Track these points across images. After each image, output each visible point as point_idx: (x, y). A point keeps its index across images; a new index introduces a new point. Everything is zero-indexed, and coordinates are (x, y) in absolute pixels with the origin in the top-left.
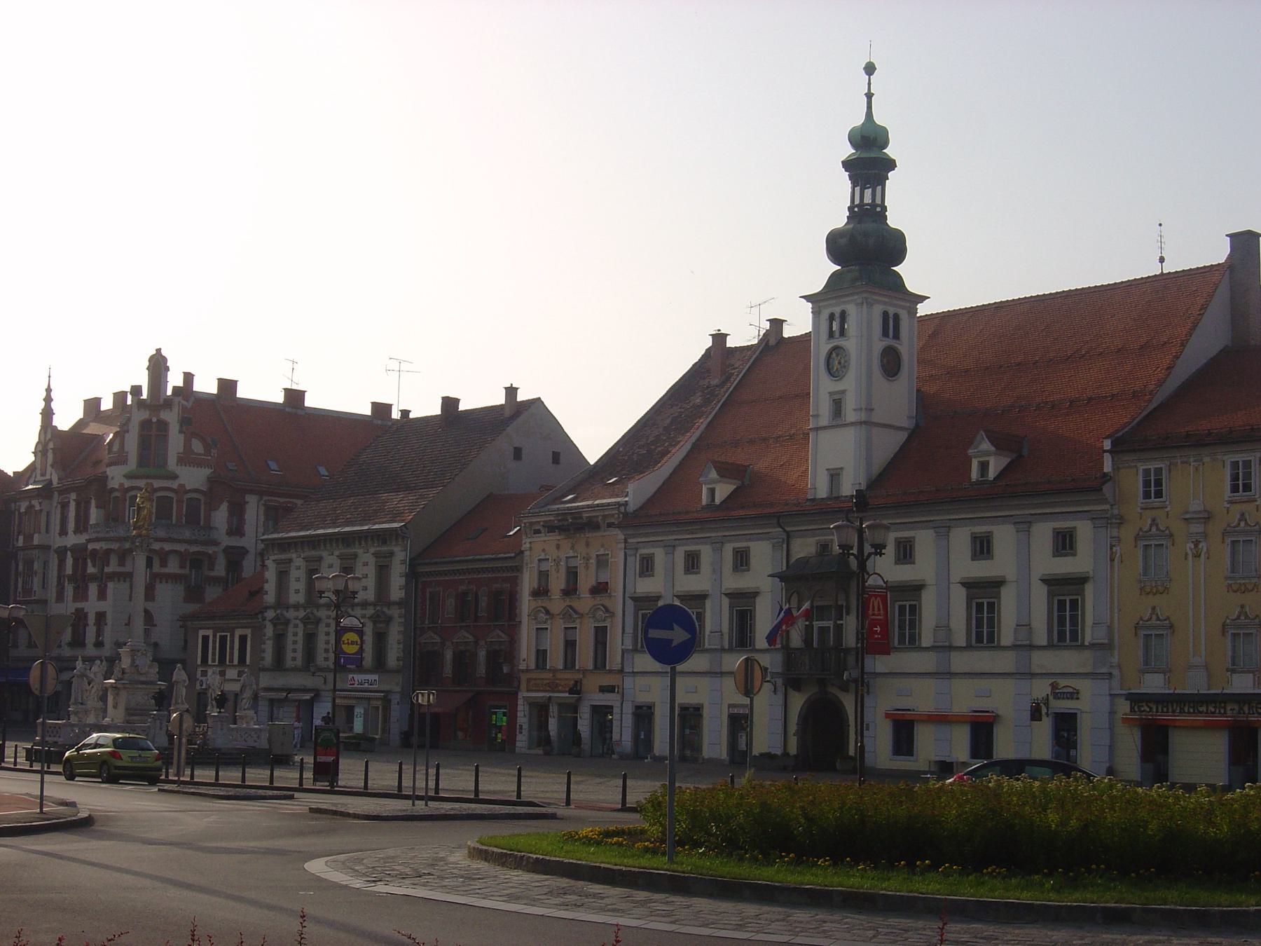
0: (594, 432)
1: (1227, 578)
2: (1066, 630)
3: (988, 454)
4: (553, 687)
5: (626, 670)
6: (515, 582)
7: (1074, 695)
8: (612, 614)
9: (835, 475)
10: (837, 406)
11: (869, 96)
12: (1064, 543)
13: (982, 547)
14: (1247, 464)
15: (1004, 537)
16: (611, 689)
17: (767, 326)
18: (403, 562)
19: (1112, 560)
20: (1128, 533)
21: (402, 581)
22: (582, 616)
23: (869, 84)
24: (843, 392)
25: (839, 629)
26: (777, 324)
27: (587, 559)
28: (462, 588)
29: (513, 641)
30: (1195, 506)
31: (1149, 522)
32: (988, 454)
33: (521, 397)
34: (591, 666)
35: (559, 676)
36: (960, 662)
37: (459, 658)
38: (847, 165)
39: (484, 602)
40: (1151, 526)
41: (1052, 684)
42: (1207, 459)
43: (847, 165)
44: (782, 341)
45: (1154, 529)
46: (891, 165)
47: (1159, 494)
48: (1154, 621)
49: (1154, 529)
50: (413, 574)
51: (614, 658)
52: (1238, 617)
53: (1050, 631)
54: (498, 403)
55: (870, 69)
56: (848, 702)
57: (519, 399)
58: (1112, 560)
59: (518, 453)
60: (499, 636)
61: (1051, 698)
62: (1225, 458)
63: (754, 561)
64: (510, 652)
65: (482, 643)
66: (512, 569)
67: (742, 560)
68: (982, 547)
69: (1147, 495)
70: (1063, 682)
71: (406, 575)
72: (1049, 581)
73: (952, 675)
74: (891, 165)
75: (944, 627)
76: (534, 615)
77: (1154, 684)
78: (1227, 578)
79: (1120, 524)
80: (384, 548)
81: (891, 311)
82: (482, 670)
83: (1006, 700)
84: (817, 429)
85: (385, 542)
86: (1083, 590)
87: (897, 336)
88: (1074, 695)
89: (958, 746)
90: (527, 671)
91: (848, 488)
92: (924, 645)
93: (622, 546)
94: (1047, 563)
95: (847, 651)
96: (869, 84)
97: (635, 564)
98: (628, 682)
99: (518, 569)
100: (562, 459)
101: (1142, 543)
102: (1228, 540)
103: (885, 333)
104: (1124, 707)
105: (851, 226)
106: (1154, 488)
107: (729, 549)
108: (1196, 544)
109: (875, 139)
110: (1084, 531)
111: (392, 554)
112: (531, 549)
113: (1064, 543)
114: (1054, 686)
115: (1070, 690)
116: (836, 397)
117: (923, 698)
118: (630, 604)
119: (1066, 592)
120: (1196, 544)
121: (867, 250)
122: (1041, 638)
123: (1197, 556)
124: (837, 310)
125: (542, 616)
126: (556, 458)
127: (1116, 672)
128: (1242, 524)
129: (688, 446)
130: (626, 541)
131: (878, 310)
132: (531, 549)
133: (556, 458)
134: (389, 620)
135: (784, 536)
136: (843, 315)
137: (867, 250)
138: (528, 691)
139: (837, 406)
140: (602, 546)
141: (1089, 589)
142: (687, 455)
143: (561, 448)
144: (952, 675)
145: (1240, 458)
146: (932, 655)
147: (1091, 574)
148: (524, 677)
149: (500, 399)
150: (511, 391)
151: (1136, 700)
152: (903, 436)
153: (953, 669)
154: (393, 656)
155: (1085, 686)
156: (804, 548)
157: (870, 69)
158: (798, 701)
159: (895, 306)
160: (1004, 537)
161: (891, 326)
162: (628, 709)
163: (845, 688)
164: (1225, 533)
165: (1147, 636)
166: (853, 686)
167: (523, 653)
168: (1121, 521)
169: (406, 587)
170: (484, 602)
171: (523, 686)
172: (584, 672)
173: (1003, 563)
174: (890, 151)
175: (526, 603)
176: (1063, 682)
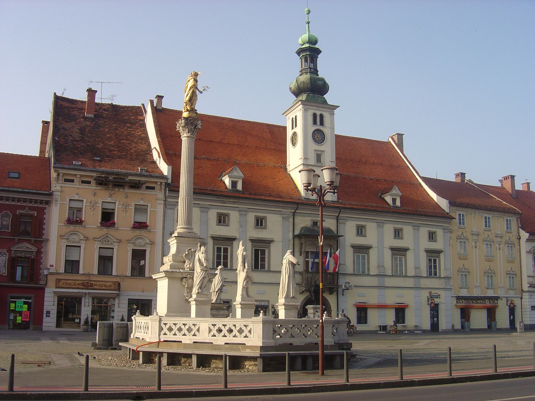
2: (433, 271)
3: (397, 195)
4: (87, 285)
7: (438, 296)
8: (152, 243)
11: (308, 23)
13: (398, 234)
15: (408, 230)
20: (454, 236)
24: (323, 151)
27: (126, 207)
30: (475, 230)
31: (461, 233)
32: (397, 195)
34: (129, 273)
35: (93, 278)
42: (477, 214)
48: (464, 270)
66: (41, 202)
68: (398, 234)
70: (434, 292)
72: (428, 251)
75: (380, 266)
77: (464, 293)
83: (407, 298)
88: (438, 296)
89: (389, 318)
93: (162, 202)
94: (425, 244)
104: (454, 301)
107: (251, 217)
108: (476, 243)
110: (440, 233)
114: (430, 293)
116: (318, 152)
117: (371, 297)
119: (433, 255)
120: (476, 243)
122: (424, 274)
124: (318, 113)
136: (321, 116)
138: (57, 288)
141: (442, 255)
151: (459, 298)
155: (442, 293)
156: (304, 221)
160: (408, 230)
165: (510, 277)
173: (406, 242)
176: (434, 292)
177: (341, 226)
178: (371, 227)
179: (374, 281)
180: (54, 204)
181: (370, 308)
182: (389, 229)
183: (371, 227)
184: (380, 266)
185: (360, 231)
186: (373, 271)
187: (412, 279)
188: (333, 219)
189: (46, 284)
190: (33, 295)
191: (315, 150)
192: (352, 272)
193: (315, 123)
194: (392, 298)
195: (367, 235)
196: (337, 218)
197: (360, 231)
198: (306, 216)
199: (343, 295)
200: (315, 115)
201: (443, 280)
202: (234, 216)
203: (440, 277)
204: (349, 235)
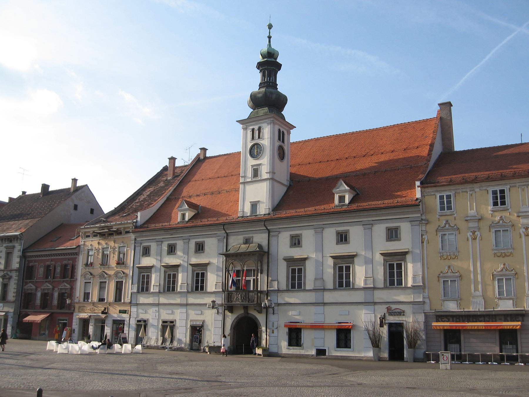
0: (109, 200)
1: (493, 250)
3: (345, 191)
5: (133, 302)
6: (75, 260)
7: (401, 313)
9: (254, 205)
10: (256, 172)
11: (270, 37)
12: (393, 234)
14: (502, 192)
16: (125, 312)
17: (199, 151)
18: (19, 251)
19: (422, 242)
20: (431, 228)
21: (18, 260)
22: (110, 276)
23: (270, 33)
24: (260, 165)
25: (256, 282)
26: (204, 150)
28: (48, 263)
29: (72, 289)
31: (444, 222)
33: (79, 184)
36: (329, 297)
37: (45, 296)
38: (260, 65)
39: (58, 270)
40: (445, 224)
41: (387, 308)
43: (260, 65)
44: (206, 158)
45: (447, 226)
46: (279, 66)
47: (449, 208)
48: (449, 274)
49: (447, 226)
50: (24, 256)
51: (126, 298)
52: (502, 270)
53: (385, 280)
54: (67, 187)
55: (270, 27)
56: (261, 318)
57: (78, 185)
58: (422, 242)
59: (76, 207)
60: (65, 286)
61: (387, 315)
62: (488, 189)
63: (206, 248)
64: (71, 294)
65: (56, 289)
67: (200, 248)
69: (442, 209)
70: (394, 307)
71: (21, 257)
73: (324, 304)
74: (279, 66)
75: (319, 278)
76: (84, 276)
78: (493, 250)
79: (427, 223)
80: (11, 244)
81: (282, 130)
82: (55, 302)
84: (244, 183)
85: (11, 241)
86: (405, 258)
87: (283, 142)
88: (401, 313)
89: (329, 340)
90: (79, 302)
91: (263, 210)
92: (307, 288)
93: (134, 242)
95: (261, 292)
96: (270, 33)
97: (140, 250)
98: (134, 309)
99: (77, 254)
100: (95, 212)
101: (440, 234)
102: (493, 230)
103: (279, 139)
105: (263, 90)
106: (446, 205)
108: (474, 233)
109: (274, 54)
110: (405, 228)
111: (14, 247)
112: (84, 244)
113: (393, 234)
114: (388, 309)
115: (399, 311)
116: (255, 167)
118: (136, 271)
120: (474, 233)
121: (269, 102)
123: (475, 239)
124: (256, 127)
125: (89, 276)
126: (92, 211)
127: (427, 301)
128: (501, 222)
129: (165, 199)
130: (135, 239)
131: (277, 127)
132: (84, 244)
133: (92, 211)
134: (10, 278)
135: (225, 235)
136: (259, 129)
137: (269, 102)
139: (256, 172)
140: (123, 242)
142: (165, 201)
143: (94, 208)
144: (324, 304)
145: (498, 189)
146: (313, 294)
147: (411, 250)
148: (77, 306)
149: (68, 185)
150: (75, 181)
152: (285, 189)
153: (326, 301)
154: (11, 295)
157: (270, 27)
158: (231, 318)
159: (283, 127)
160: (356, 233)
161: (282, 136)
162: (133, 323)
163: (260, 312)
164: (490, 227)
166: (265, 310)
167: (78, 294)
168: (428, 222)
169: (20, 263)
170: (58, 270)
171: (76, 310)
172: (110, 304)
174: (279, 60)
175: (80, 269)
177: (273, 240)
178: (308, 236)
179: (310, 297)
180: (80, 255)
181: (304, 328)
182: (330, 234)
183: (308, 236)
184: (319, 278)
185: (296, 242)
186: (309, 284)
187: (362, 292)
188: (265, 233)
189: (74, 310)
190: (67, 318)
191: (252, 166)
192: (285, 288)
193: (253, 138)
194: (334, 316)
195: (303, 246)
196: (269, 232)
197: (296, 242)
198: (238, 235)
199: (273, 313)
200: (253, 130)
201: (409, 291)
202: (180, 244)
203: (406, 288)
204: (283, 248)
